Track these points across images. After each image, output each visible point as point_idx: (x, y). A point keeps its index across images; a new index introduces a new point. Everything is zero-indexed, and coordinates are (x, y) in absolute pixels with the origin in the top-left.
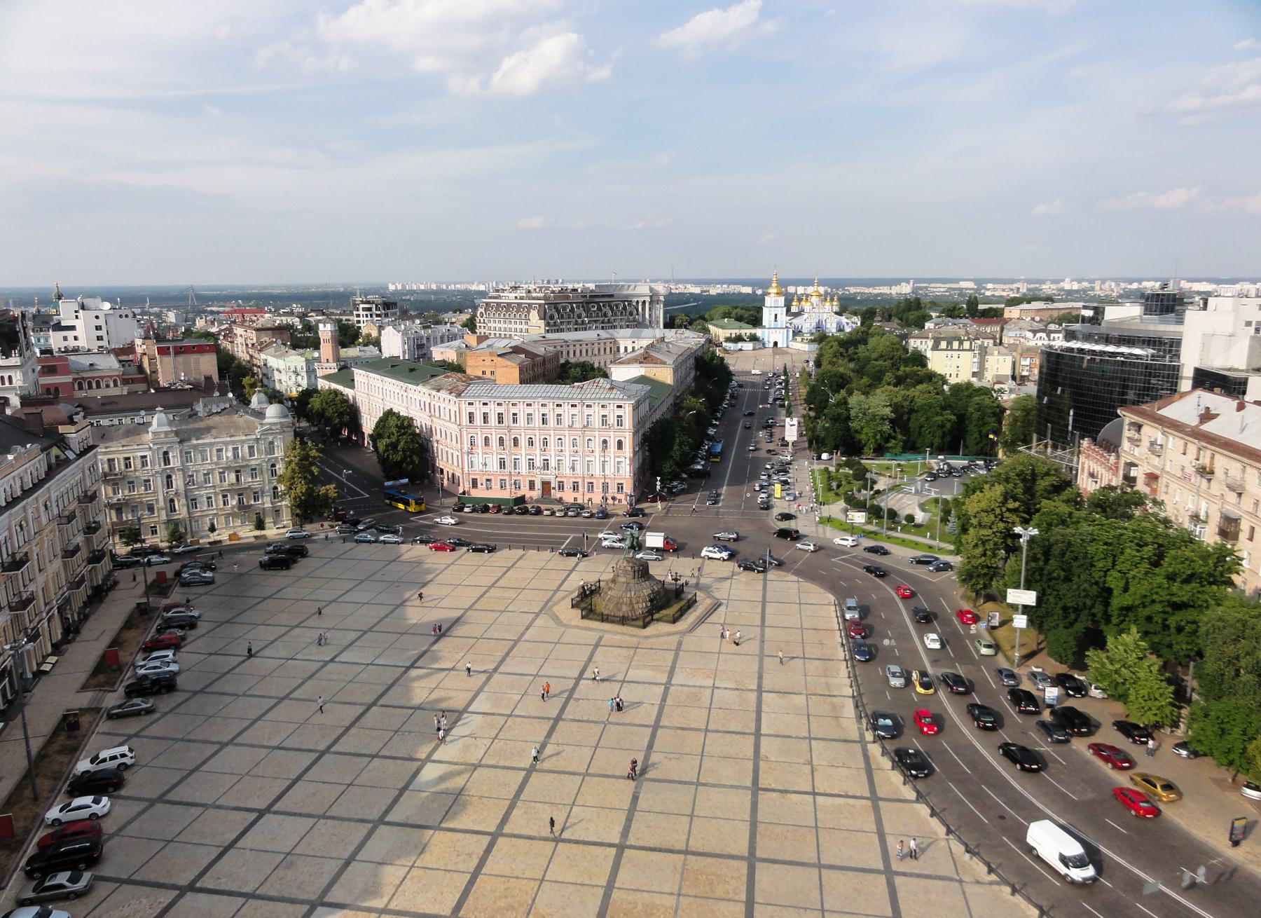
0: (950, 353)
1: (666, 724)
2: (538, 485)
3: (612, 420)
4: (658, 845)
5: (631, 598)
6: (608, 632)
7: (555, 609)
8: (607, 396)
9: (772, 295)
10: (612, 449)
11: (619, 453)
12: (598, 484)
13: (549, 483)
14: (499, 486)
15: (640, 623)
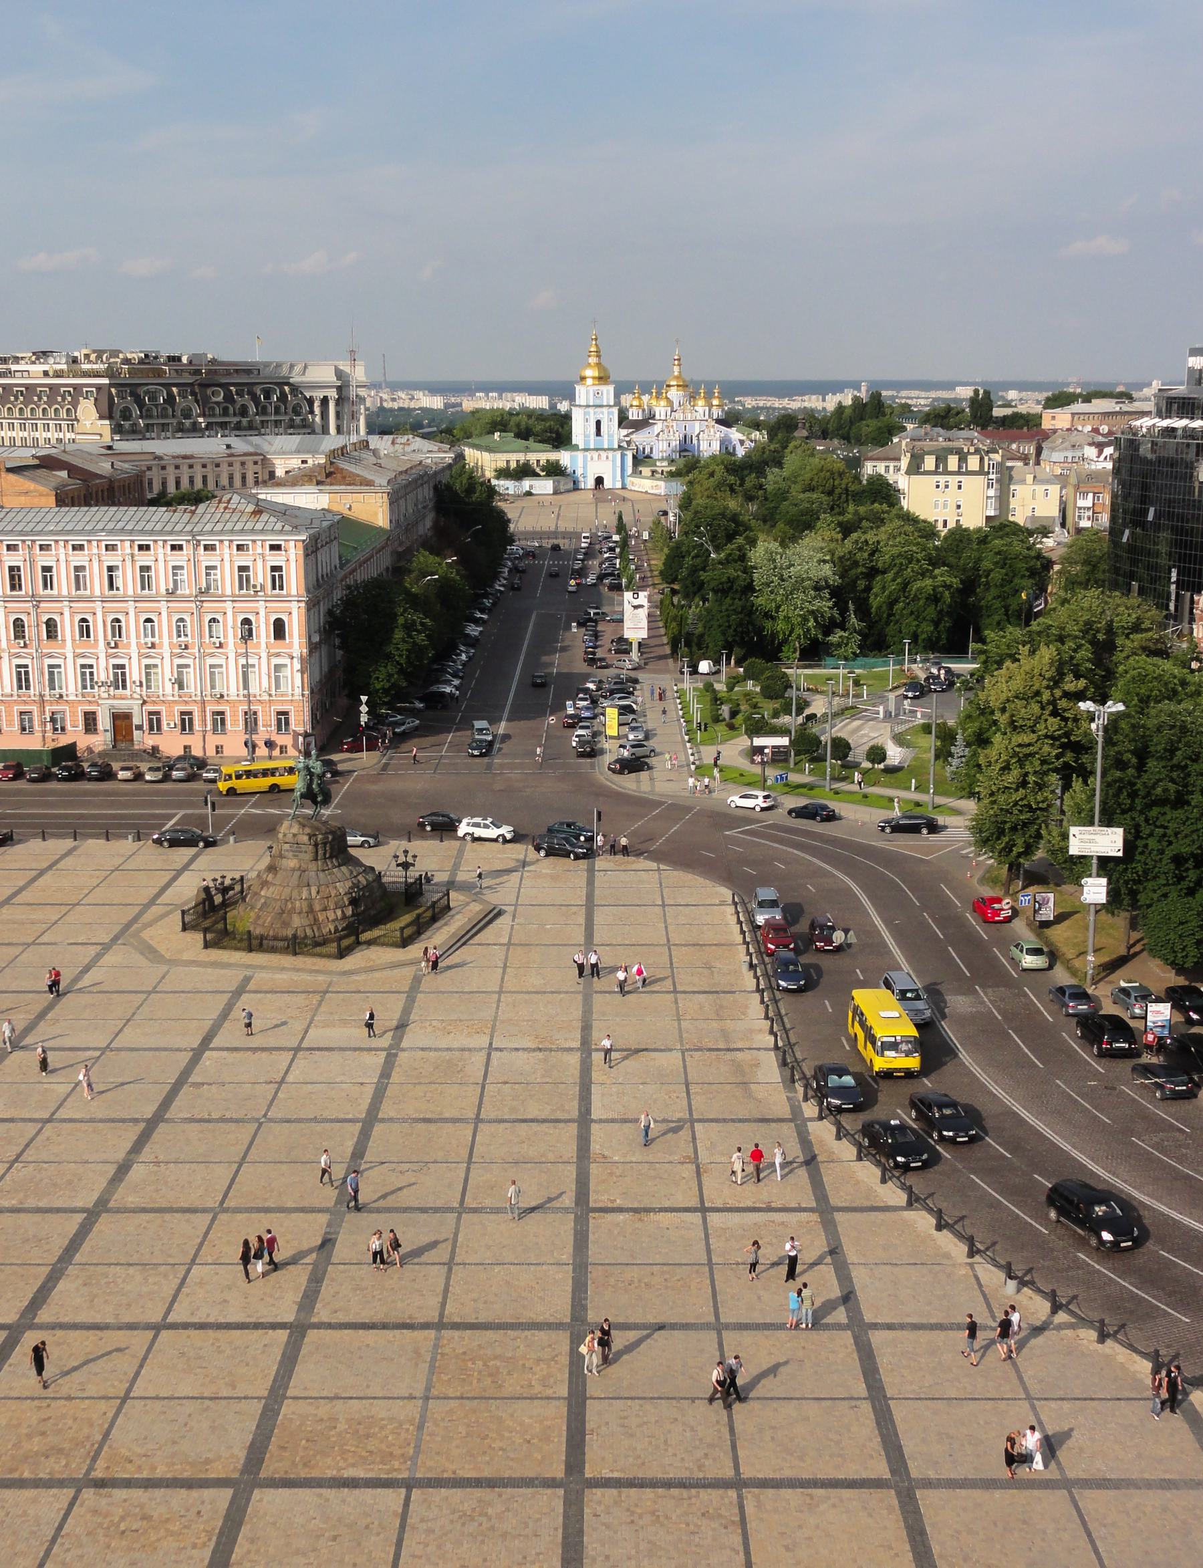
0: (942, 479)
1: (392, 1114)
2: (104, 722)
3: (261, 576)
4: (378, 1318)
5: (310, 900)
6: (262, 968)
7: (146, 935)
8: (249, 526)
9: (589, 382)
10: (263, 640)
11: (279, 646)
12: (234, 714)
13: (127, 717)
14: (17, 727)
15: (332, 948)
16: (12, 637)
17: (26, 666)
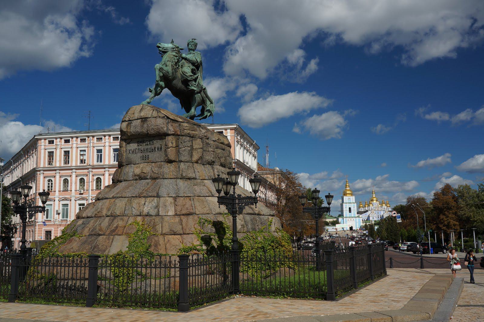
16: (78, 189)
17: (84, 205)
